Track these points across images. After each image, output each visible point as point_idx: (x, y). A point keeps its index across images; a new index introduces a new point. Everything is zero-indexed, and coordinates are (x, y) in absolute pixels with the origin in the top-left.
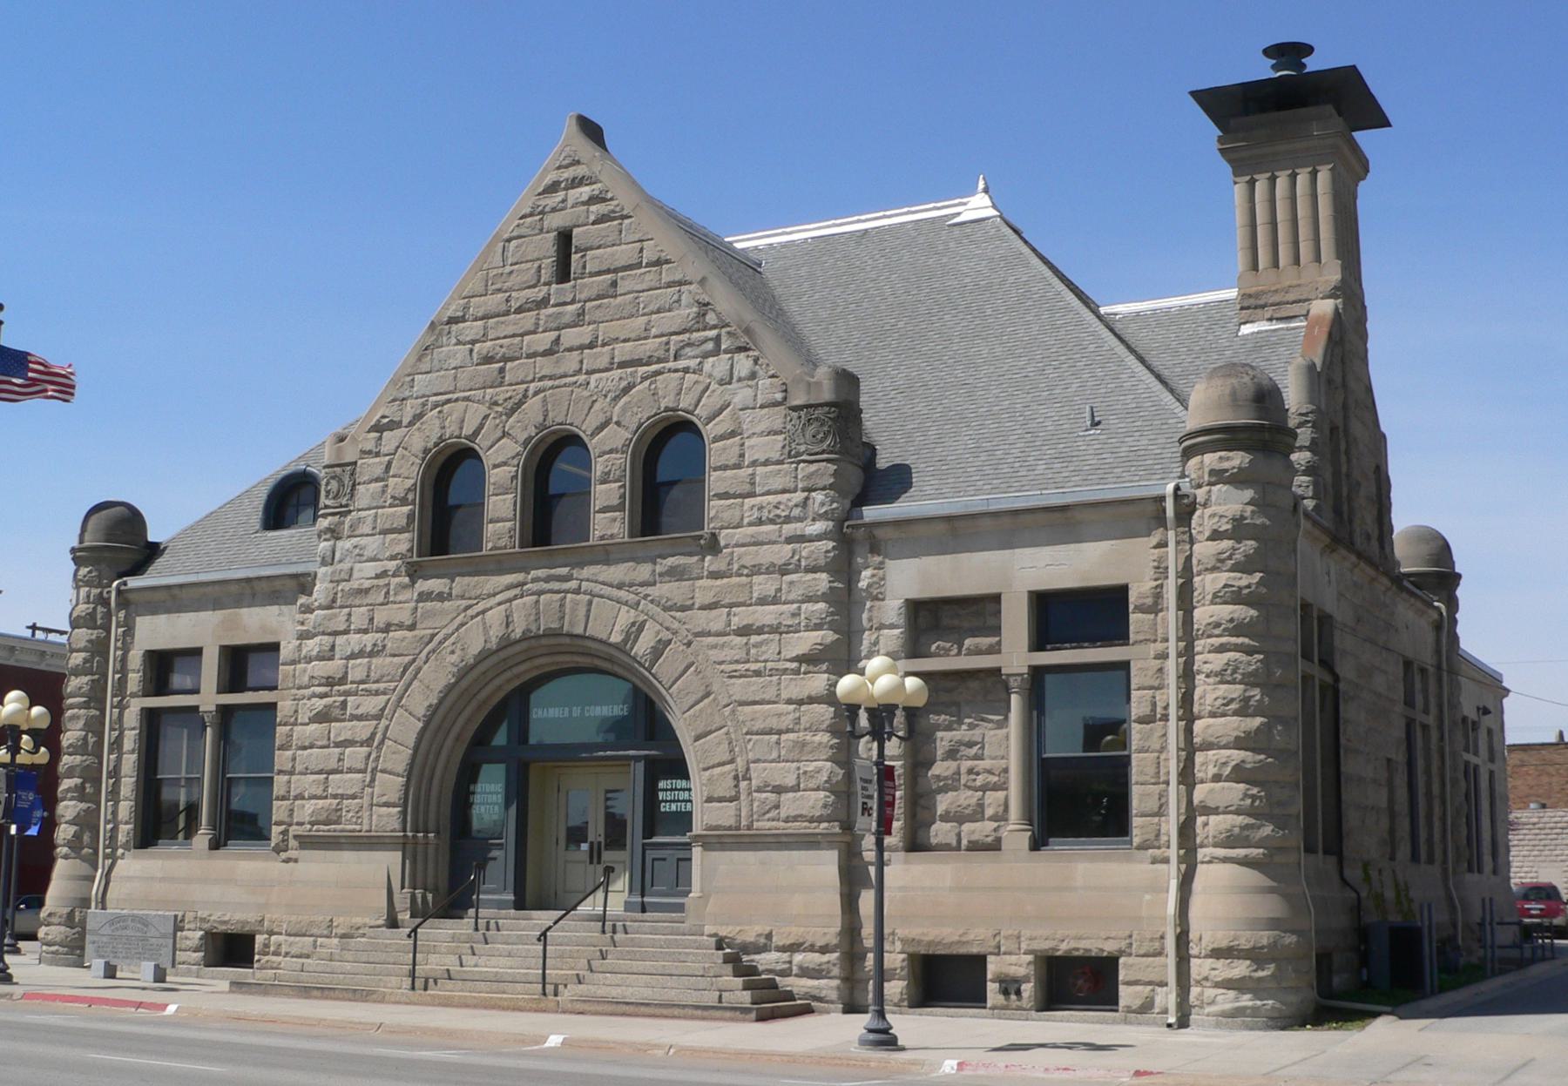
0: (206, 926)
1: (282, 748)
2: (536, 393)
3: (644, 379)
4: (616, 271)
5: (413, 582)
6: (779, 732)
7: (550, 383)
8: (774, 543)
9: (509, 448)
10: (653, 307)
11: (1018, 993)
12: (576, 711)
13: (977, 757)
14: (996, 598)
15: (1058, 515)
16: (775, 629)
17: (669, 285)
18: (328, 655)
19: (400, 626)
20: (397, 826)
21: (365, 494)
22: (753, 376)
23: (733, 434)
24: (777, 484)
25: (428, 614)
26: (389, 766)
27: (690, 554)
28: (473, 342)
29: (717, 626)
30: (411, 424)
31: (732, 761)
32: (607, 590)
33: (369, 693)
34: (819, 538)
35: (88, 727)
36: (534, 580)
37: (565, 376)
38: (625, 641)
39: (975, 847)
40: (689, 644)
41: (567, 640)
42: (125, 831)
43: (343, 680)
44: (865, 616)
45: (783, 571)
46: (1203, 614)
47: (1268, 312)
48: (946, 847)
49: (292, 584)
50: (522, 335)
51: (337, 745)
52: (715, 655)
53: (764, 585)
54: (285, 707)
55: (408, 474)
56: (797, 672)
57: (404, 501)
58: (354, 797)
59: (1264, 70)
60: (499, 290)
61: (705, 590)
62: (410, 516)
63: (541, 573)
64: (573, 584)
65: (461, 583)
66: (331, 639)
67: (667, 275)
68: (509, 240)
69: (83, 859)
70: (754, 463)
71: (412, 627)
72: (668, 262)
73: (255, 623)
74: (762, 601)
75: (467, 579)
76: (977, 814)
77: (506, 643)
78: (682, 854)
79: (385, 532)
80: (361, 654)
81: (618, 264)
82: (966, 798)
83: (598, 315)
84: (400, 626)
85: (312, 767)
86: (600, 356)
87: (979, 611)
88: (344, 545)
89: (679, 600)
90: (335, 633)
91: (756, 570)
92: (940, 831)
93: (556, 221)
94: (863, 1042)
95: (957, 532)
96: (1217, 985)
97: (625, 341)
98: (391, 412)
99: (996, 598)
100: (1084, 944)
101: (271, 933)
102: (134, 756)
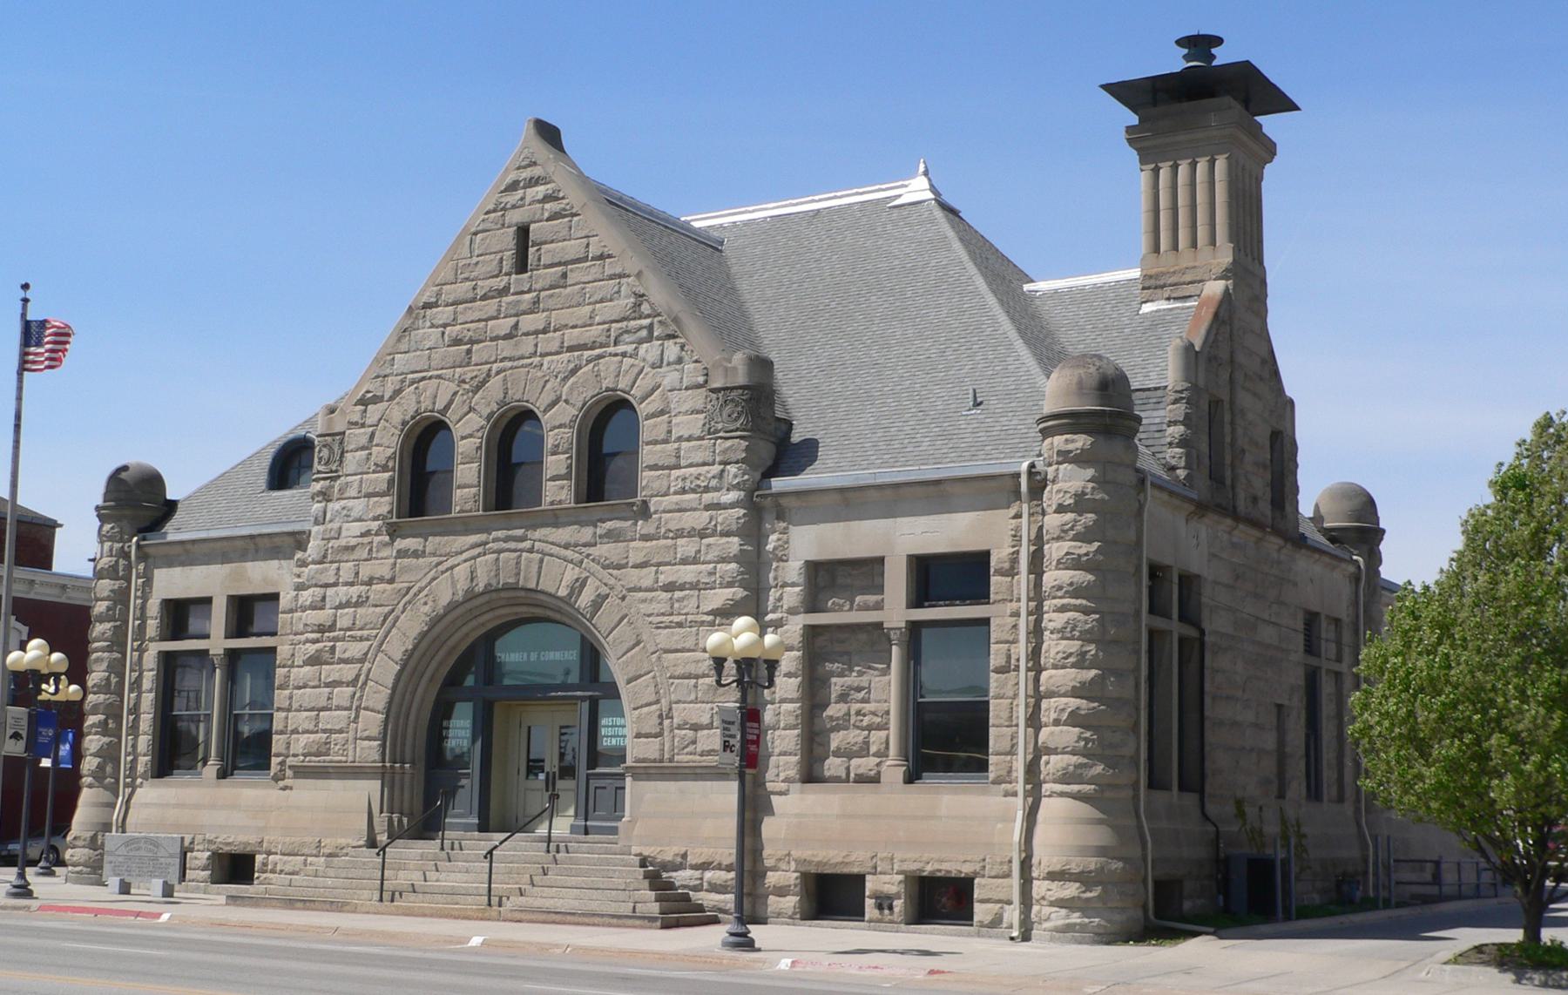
0: (213, 847)
1: (281, 687)
2: (498, 373)
3: (589, 362)
4: (565, 264)
5: (393, 541)
6: (697, 677)
7: (509, 364)
8: (695, 510)
9: (475, 422)
10: (597, 297)
11: (891, 908)
12: (533, 656)
13: (864, 701)
14: (881, 560)
15: (932, 488)
16: (695, 586)
17: (611, 277)
18: (319, 605)
19: (381, 580)
20: (377, 757)
21: (352, 460)
22: (680, 361)
23: (662, 413)
24: (698, 457)
25: (405, 570)
26: (371, 704)
27: (625, 519)
28: (445, 326)
29: (647, 583)
30: (391, 399)
31: (658, 702)
32: (555, 550)
33: (354, 638)
34: (732, 506)
35: (110, 669)
36: (495, 540)
37: (522, 358)
38: (570, 595)
39: (861, 779)
40: (623, 598)
41: (523, 594)
42: (144, 762)
43: (332, 628)
44: (771, 575)
45: (702, 535)
46: (1051, 577)
47: (1167, 292)
48: (837, 780)
49: (290, 540)
50: (486, 320)
51: (327, 685)
52: (644, 608)
53: (686, 547)
54: (283, 651)
55: (389, 444)
56: (712, 624)
57: (385, 469)
58: (341, 731)
59: (1174, 62)
60: (467, 279)
61: (638, 550)
62: (391, 482)
63: (500, 534)
64: (527, 544)
65: (433, 541)
66: (321, 591)
67: (610, 267)
68: (475, 234)
69: (106, 788)
70: (680, 439)
71: (391, 581)
72: (610, 256)
73: (258, 575)
74: (684, 562)
75: (438, 539)
76: (863, 750)
77: (471, 596)
78: (618, 784)
79: (369, 495)
80: (348, 604)
81: (568, 258)
82: (854, 736)
83: (551, 303)
84: (381, 580)
86: (550, 341)
87: (867, 571)
88: (334, 506)
89: (615, 559)
90: (326, 586)
91: (679, 534)
92: (833, 766)
93: (515, 217)
94: (725, 944)
95: (850, 502)
96: (1052, 904)
97: (574, 327)
98: (374, 387)
99: (881, 560)
100: (945, 866)
101: (269, 853)
102: (152, 695)
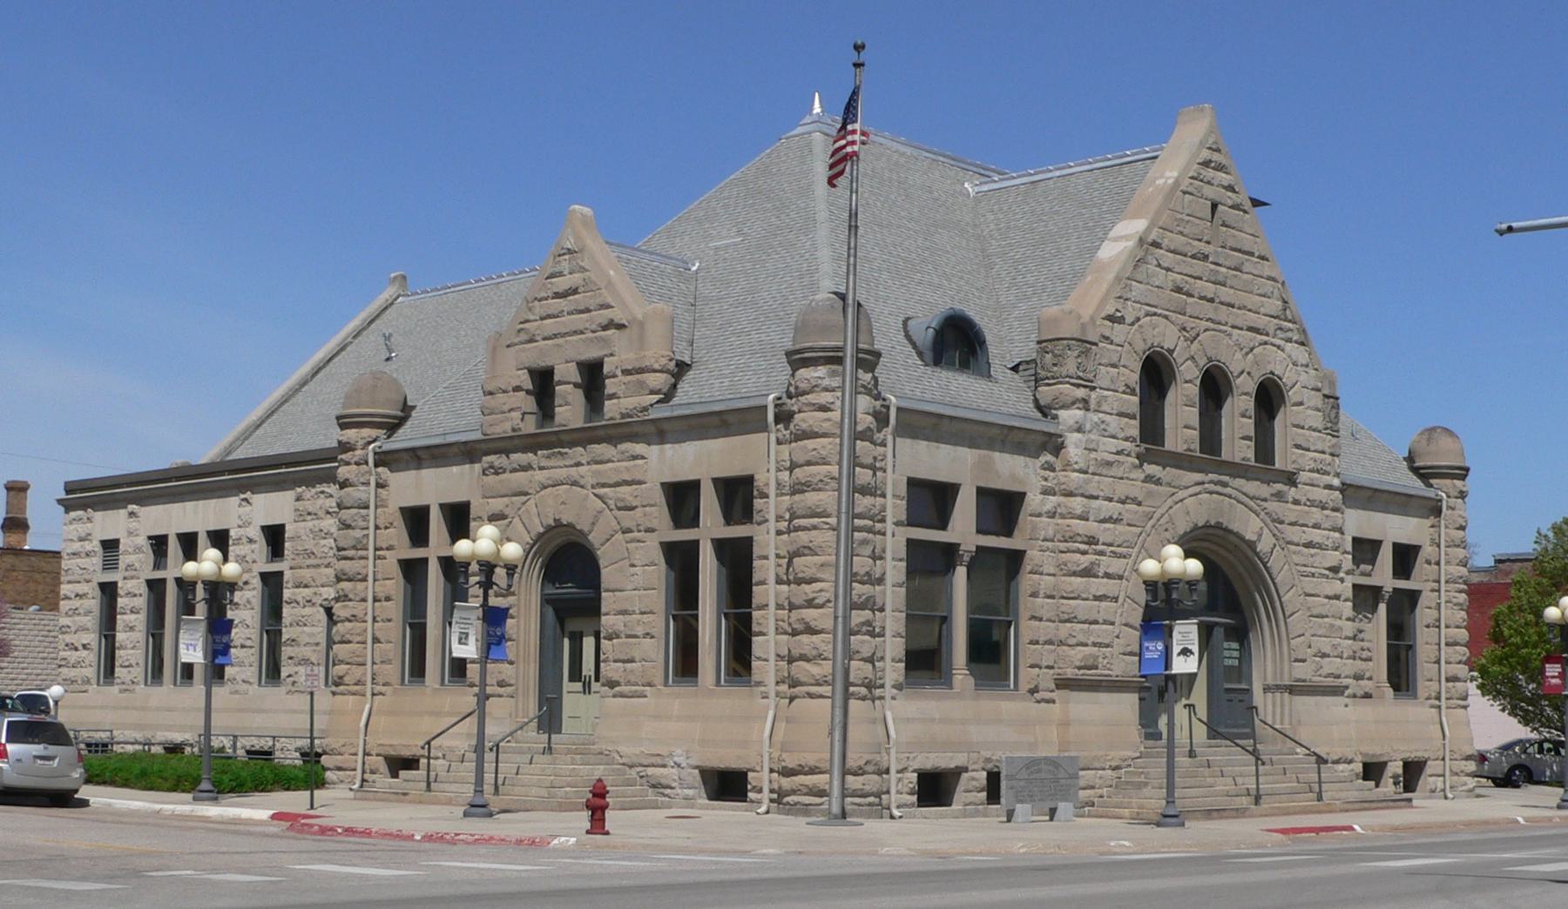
0: (989, 766)
14: (1380, 542)
17: (1269, 278)
28: (1168, 269)
30: (1132, 324)
33: (1115, 555)
36: (1211, 482)
52: (1296, 559)
53: (1316, 515)
54: (1033, 556)
58: (1107, 646)
60: (1181, 233)
61: (1289, 511)
64: (1228, 490)
71: (1139, 504)
73: (1011, 470)
85: (1081, 617)
91: (1312, 503)
99: (1380, 542)
